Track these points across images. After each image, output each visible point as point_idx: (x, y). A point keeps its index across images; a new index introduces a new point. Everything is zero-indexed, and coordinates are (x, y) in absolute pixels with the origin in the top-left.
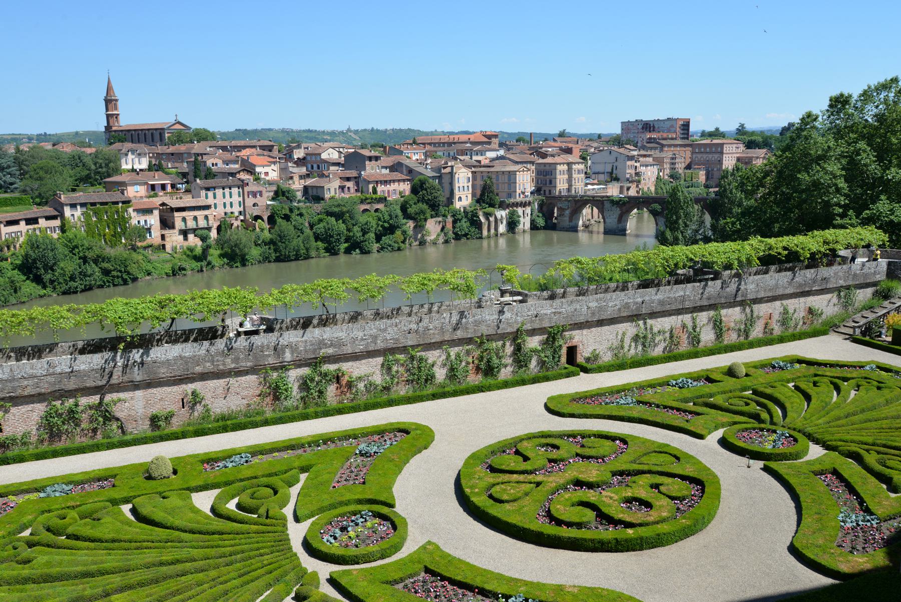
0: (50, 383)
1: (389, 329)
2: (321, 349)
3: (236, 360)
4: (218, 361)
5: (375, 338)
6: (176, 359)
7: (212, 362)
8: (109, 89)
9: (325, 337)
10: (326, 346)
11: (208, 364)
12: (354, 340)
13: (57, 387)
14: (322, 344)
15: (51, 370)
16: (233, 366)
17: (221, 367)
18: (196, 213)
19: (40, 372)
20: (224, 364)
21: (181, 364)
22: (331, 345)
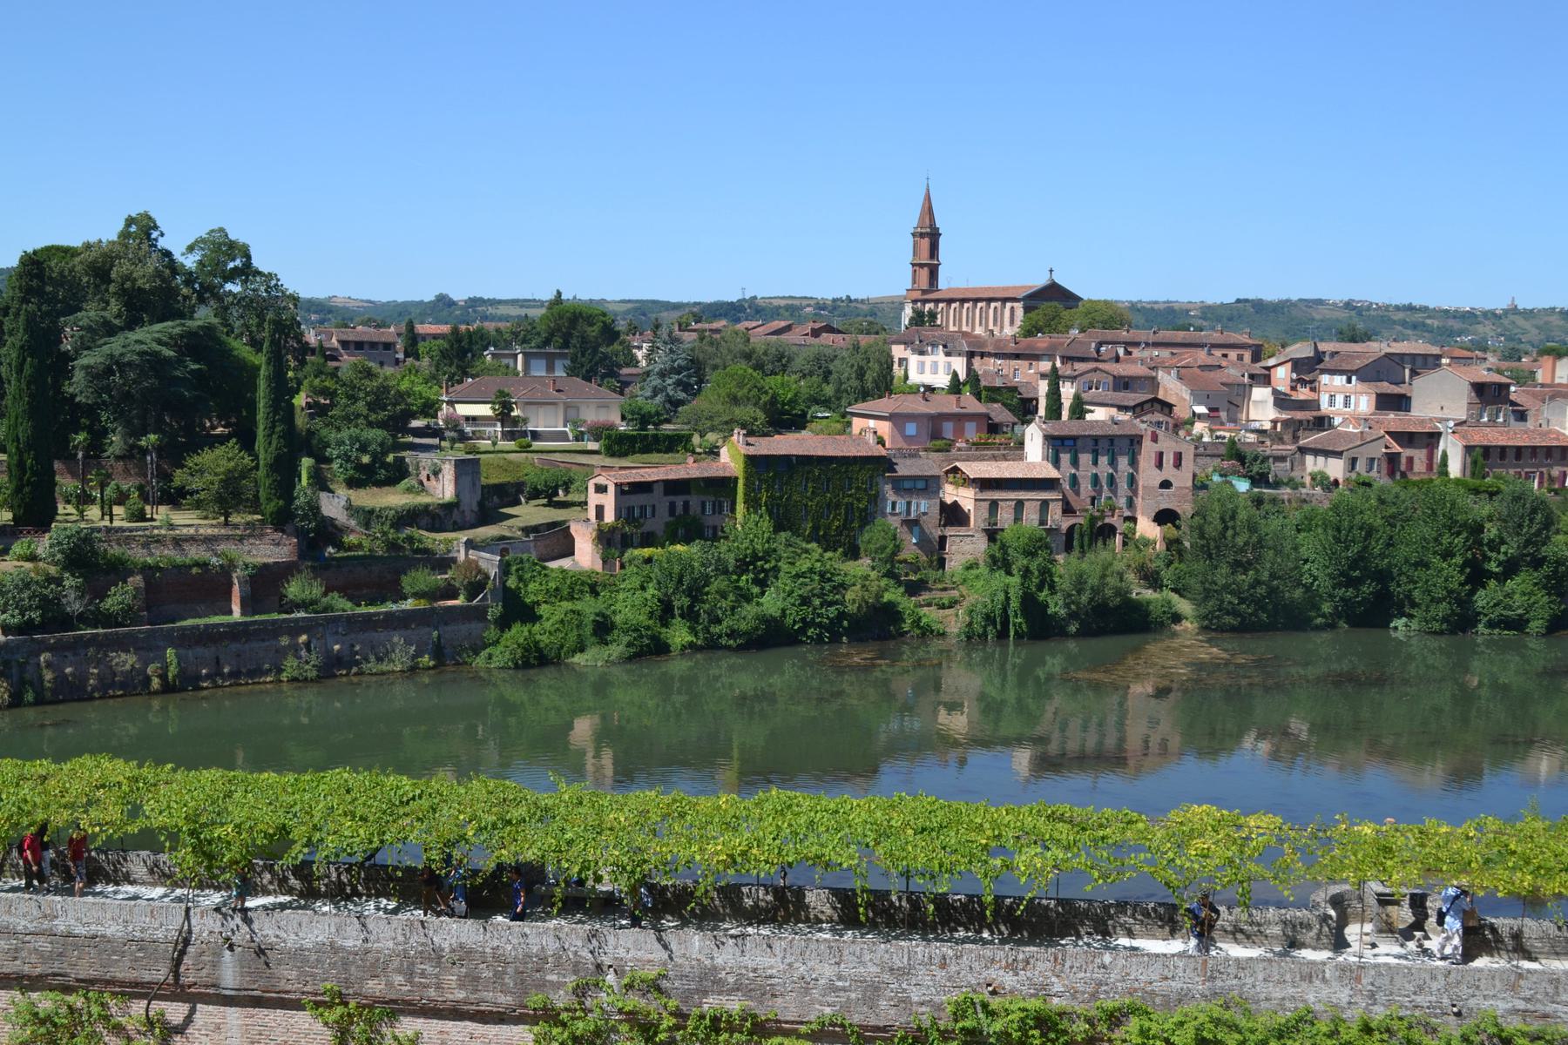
0: (41, 955)
1: (922, 971)
2: (705, 993)
3: (472, 981)
4: (423, 974)
5: (873, 991)
6: (319, 948)
7: (410, 974)
8: (928, 211)
9: (719, 961)
10: (719, 987)
11: (399, 979)
12: (805, 986)
13: (56, 967)
14: (709, 980)
15: (46, 925)
16: (461, 995)
17: (432, 993)
18: (1022, 495)
19: (22, 924)
20: (438, 987)
21: (333, 965)
22: (737, 988)
